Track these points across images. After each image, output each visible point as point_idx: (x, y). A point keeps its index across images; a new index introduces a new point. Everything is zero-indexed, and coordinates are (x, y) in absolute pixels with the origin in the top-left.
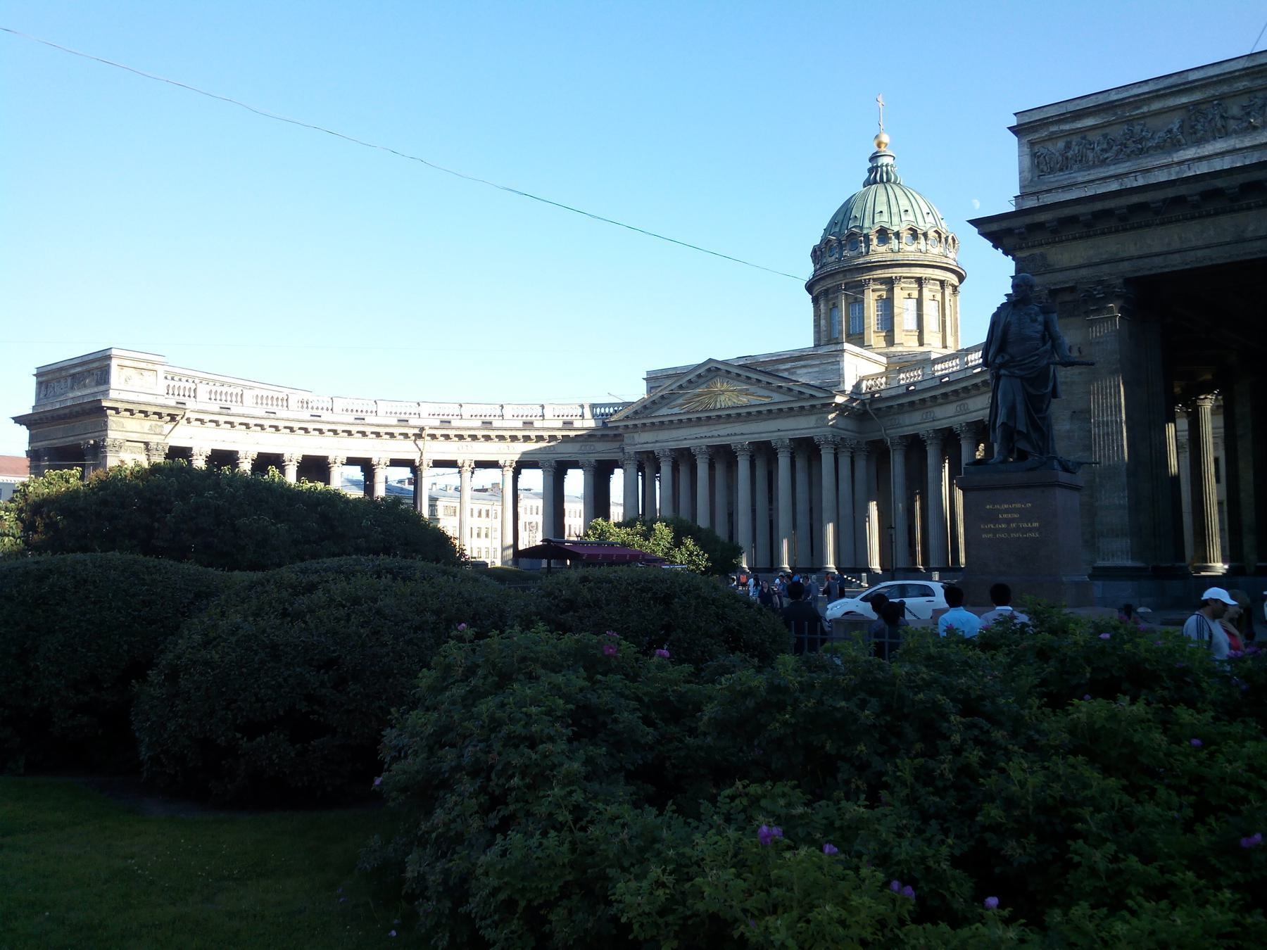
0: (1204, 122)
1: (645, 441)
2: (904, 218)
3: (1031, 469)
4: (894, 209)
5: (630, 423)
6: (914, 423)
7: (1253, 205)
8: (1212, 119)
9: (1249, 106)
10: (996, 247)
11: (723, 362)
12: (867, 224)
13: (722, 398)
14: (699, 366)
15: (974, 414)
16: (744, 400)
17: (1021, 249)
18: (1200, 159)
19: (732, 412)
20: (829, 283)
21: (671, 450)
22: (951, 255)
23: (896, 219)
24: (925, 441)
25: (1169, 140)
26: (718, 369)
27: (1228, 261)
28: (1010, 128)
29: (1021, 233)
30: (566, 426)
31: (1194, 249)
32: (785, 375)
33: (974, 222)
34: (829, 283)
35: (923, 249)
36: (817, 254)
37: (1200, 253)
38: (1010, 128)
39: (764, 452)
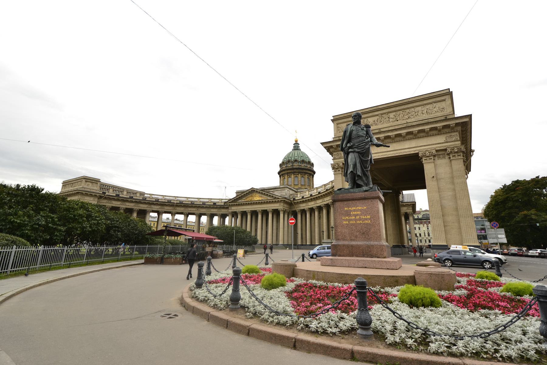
1: (234, 209)
3: (366, 191)
4: (299, 156)
5: (231, 204)
6: (303, 206)
11: (256, 189)
12: (293, 159)
13: (255, 198)
14: (248, 190)
16: (261, 199)
19: (258, 202)
20: (283, 173)
21: (241, 211)
23: (299, 158)
24: (306, 211)
26: (254, 190)
28: (331, 120)
30: (214, 205)
32: (272, 193)
33: (322, 144)
34: (283, 173)
36: (281, 165)
38: (331, 120)
39: (265, 213)
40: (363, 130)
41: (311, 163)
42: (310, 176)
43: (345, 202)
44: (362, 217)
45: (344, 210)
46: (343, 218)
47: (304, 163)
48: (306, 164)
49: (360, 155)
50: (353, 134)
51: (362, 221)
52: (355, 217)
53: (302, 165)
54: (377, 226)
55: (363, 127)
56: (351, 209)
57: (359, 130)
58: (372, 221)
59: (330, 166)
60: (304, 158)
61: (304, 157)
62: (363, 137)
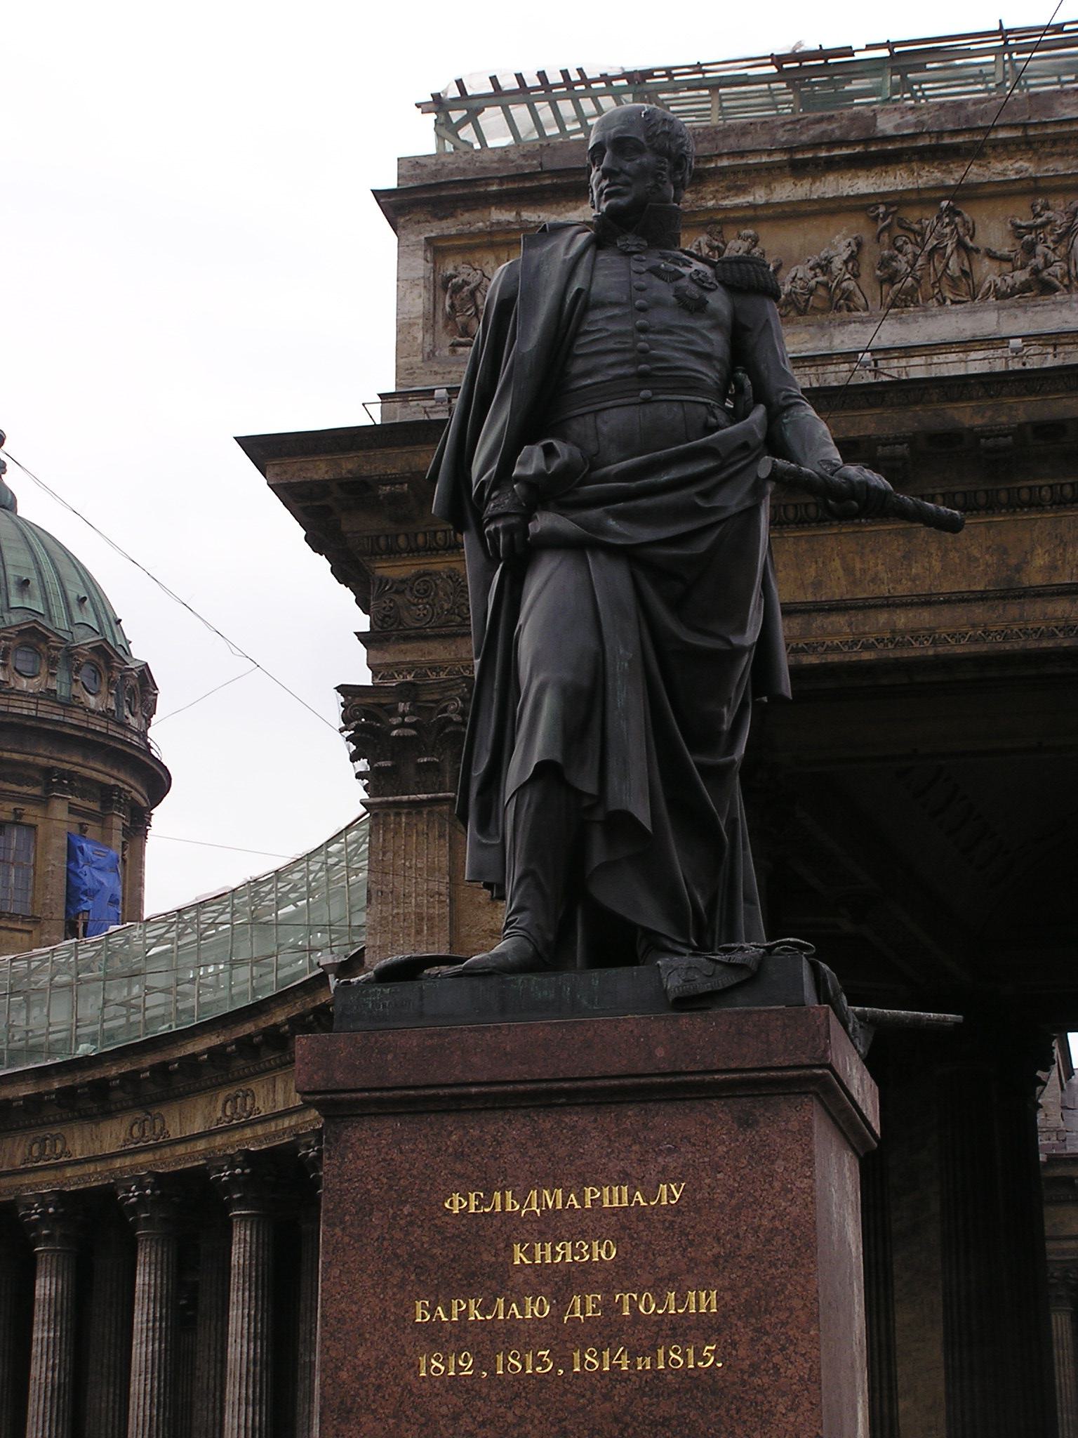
0: (916, 257)
2: (15, 602)
3: (687, 1002)
7: (1046, 493)
8: (934, 249)
9: (1030, 229)
10: (316, 542)
15: (181, 1150)
17: (392, 552)
18: (907, 351)
22: (133, 721)
25: (822, 292)
27: (983, 648)
29: (394, 499)
31: (890, 603)
35: (63, 692)
37: (902, 619)
40: (696, 307)
41: (125, 673)
42: (101, 819)
43: (449, 1121)
44: (634, 1306)
46: (421, 1315)
47: (44, 670)
48: (63, 675)
50: (583, 345)
52: (561, 1303)
53: (24, 684)
54: (793, 1408)
55: (698, 280)
56: (512, 1205)
57: (659, 303)
58: (742, 1352)
59: (334, 707)
60: (46, 600)
61: (53, 587)
62: (690, 384)
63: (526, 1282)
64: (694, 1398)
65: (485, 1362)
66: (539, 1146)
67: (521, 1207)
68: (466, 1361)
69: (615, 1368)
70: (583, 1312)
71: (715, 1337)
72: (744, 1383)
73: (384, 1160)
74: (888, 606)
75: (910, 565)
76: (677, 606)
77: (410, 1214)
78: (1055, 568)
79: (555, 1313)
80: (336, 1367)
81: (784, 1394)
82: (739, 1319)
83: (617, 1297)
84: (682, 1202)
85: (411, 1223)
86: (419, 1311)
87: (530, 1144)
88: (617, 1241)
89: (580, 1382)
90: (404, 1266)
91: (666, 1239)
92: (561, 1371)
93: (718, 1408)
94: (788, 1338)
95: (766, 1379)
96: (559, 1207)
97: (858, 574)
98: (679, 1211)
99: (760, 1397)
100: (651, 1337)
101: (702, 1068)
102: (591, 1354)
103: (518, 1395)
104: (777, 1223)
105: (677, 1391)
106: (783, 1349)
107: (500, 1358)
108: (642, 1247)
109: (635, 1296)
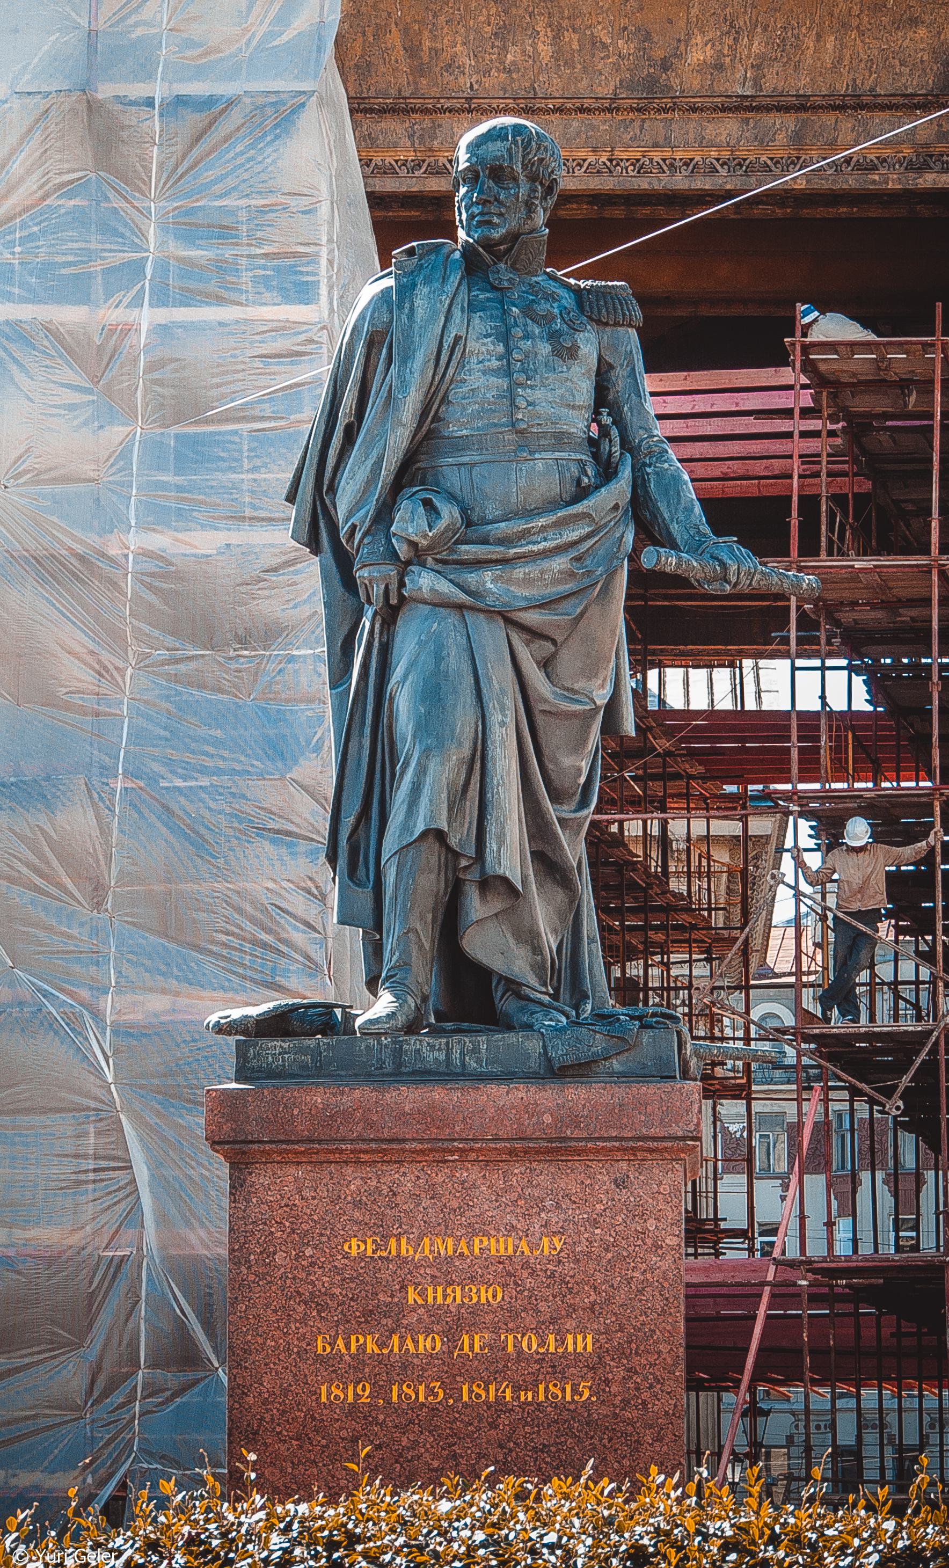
27: (607, 184)
43: (349, 1170)
45: (340, 1262)
49: (524, 654)
51: (517, 1389)
54: (659, 1439)
58: (614, 1389)
63: (419, 1320)
64: (570, 1428)
65: (381, 1390)
66: (431, 1198)
67: (415, 1252)
68: (364, 1390)
69: (500, 1400)
70: (472, 1347)
71: (590, 1375)
72: (616, 1415)
73: (286, 1205)
74: (470, 111)
75: (505, 49)
76: (546, 664)
77: (311, 1257)
78: (719, 67)
79: (445, 1349)
80: (243, 1393)
81: (651, 1426)
82: (613, 1359)
83: (503, 1337)
84: (562, 1254)
85: (313, 1264)
86: (320, 1344)
87: (423, 1195)
88: (505, 1286)
89: (468, 1411)
90: (306, 1303)
91: (548, 1287)
92: (451, 1401)
93: (592, 1438)
94: (655, 1378)
95: (635, 1414)
96: (450, 1253)
97: (426, 59)
98: (560, 1262)
99: (630, 1428)
100: (533, 1373)
101: (585, 1135)
102: (479, 1386)
103: (411, 1422)
104: (649, 1276)
105: (556, 1422)
106: (651, 1387)
107: (395, 1388)
108: (526, 1293)
109: (519, 1336)
